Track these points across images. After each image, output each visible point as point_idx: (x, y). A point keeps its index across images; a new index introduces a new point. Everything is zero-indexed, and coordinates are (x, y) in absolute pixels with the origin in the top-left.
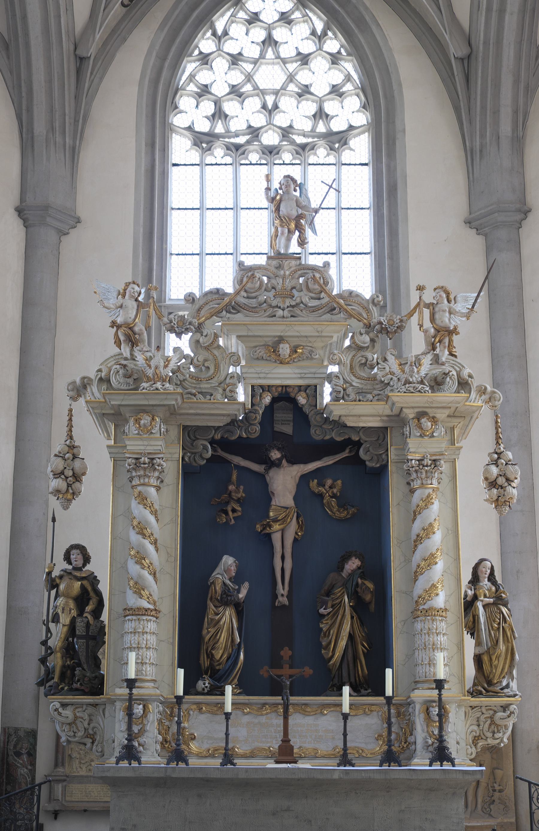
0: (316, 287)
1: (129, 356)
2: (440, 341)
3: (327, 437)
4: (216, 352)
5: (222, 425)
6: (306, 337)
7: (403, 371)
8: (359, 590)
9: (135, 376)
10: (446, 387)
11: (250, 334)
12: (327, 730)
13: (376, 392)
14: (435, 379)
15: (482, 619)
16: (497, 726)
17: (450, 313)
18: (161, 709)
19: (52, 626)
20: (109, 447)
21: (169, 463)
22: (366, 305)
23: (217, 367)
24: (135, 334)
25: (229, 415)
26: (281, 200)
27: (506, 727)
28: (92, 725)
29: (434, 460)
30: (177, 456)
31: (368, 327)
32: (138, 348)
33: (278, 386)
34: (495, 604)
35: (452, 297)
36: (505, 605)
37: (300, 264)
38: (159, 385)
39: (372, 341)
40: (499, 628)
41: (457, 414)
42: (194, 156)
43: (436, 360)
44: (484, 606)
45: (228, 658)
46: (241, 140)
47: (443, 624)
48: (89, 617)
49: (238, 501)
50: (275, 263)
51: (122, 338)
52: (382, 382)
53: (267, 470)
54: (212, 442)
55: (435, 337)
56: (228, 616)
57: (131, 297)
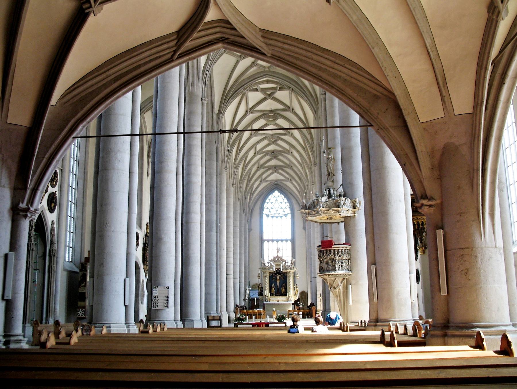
12: (282, 300)
46: (273, 215)
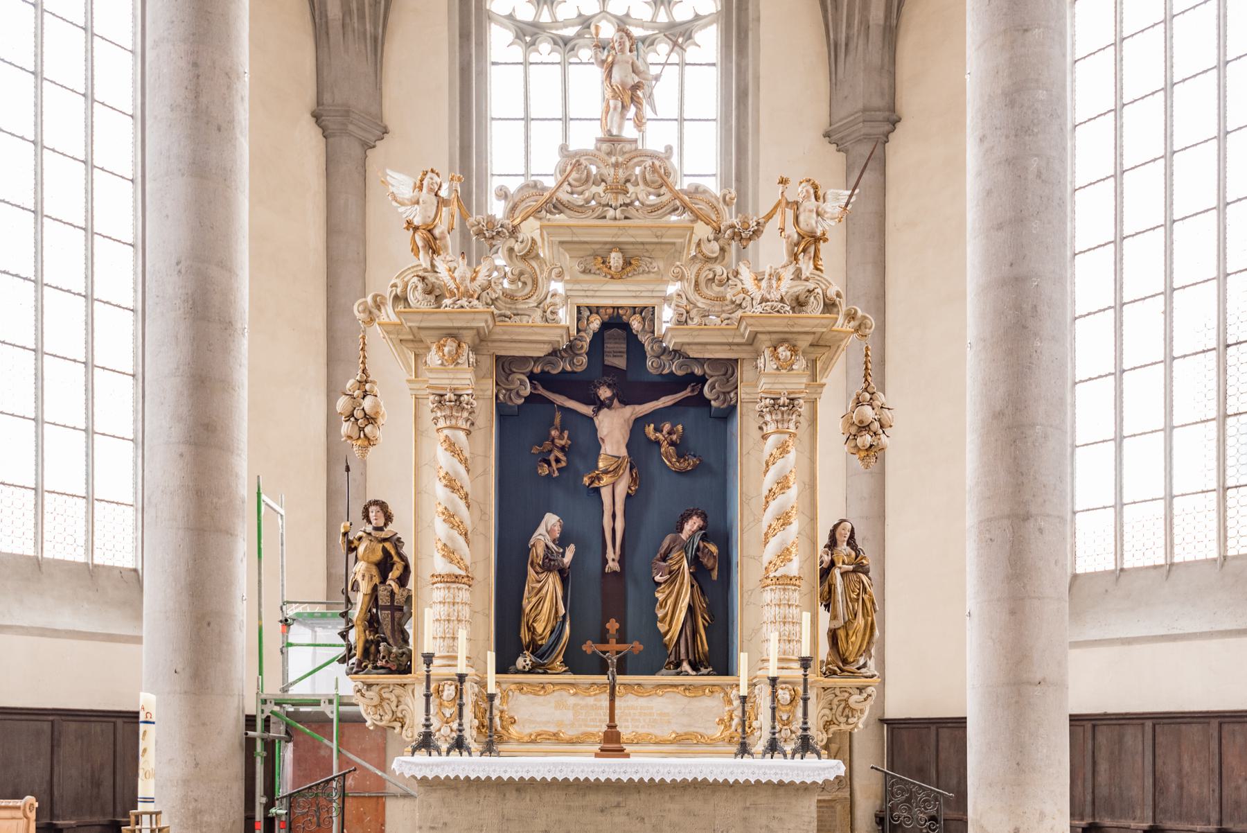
0: (656, 177)
1: (429, 268)
2: (804, 251)
3: (666, 371)
4: (534, 264)
5: (542, 355)
6: (643, 243)
7: (760, 288)
8: (700, 554)
9: (437, 292)
10: (809, 308)
11: (575, 239)
13: (724, 316)
14: (797, 298)
15: (839, 589)
16: (852, 710)
17: (818, 214)
18: (476, 690)
19: (351, 594)
20: (409, 381)
21: (481, 402)
22: (715, 203)
23: (535, 282)
24: (435, 239)
25: (550, 342)
26: (613, 63)
27: (862, 711)
28: (400, 708)
29: (792, 399)
30: (489, 393)
31: (718, 231)
32: (441, 257)
33: (606, 308)
34: (854, 571)
35: (820, 193)
36: (866, 573)
37: (636, 149)
38: (464, 302)
39: (722, 249)
40: (857, 600)
41: (821, 343)
42: (517, 53)
43: (798, 275)
44: (842, 574)
45: (552, 632)
47: (796, 594)
48: (393, 584)
49: (562, 449)
50: (605, 147)
51: (420, 244)
52: (733, 302)
53: (596, 412)
54: (532, 377)
55: (797, 244)
56: (552, 584)
57: (431, 190)
